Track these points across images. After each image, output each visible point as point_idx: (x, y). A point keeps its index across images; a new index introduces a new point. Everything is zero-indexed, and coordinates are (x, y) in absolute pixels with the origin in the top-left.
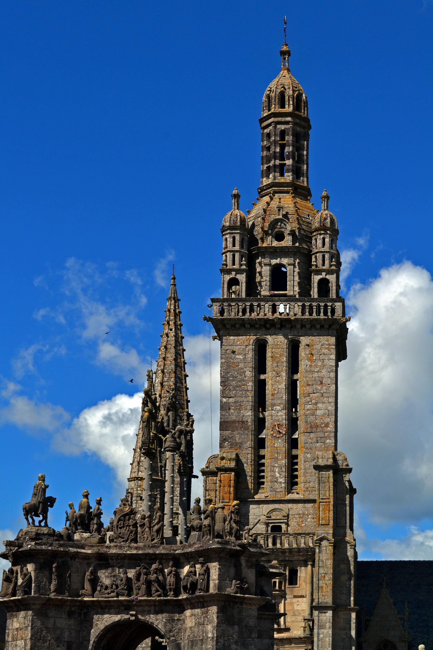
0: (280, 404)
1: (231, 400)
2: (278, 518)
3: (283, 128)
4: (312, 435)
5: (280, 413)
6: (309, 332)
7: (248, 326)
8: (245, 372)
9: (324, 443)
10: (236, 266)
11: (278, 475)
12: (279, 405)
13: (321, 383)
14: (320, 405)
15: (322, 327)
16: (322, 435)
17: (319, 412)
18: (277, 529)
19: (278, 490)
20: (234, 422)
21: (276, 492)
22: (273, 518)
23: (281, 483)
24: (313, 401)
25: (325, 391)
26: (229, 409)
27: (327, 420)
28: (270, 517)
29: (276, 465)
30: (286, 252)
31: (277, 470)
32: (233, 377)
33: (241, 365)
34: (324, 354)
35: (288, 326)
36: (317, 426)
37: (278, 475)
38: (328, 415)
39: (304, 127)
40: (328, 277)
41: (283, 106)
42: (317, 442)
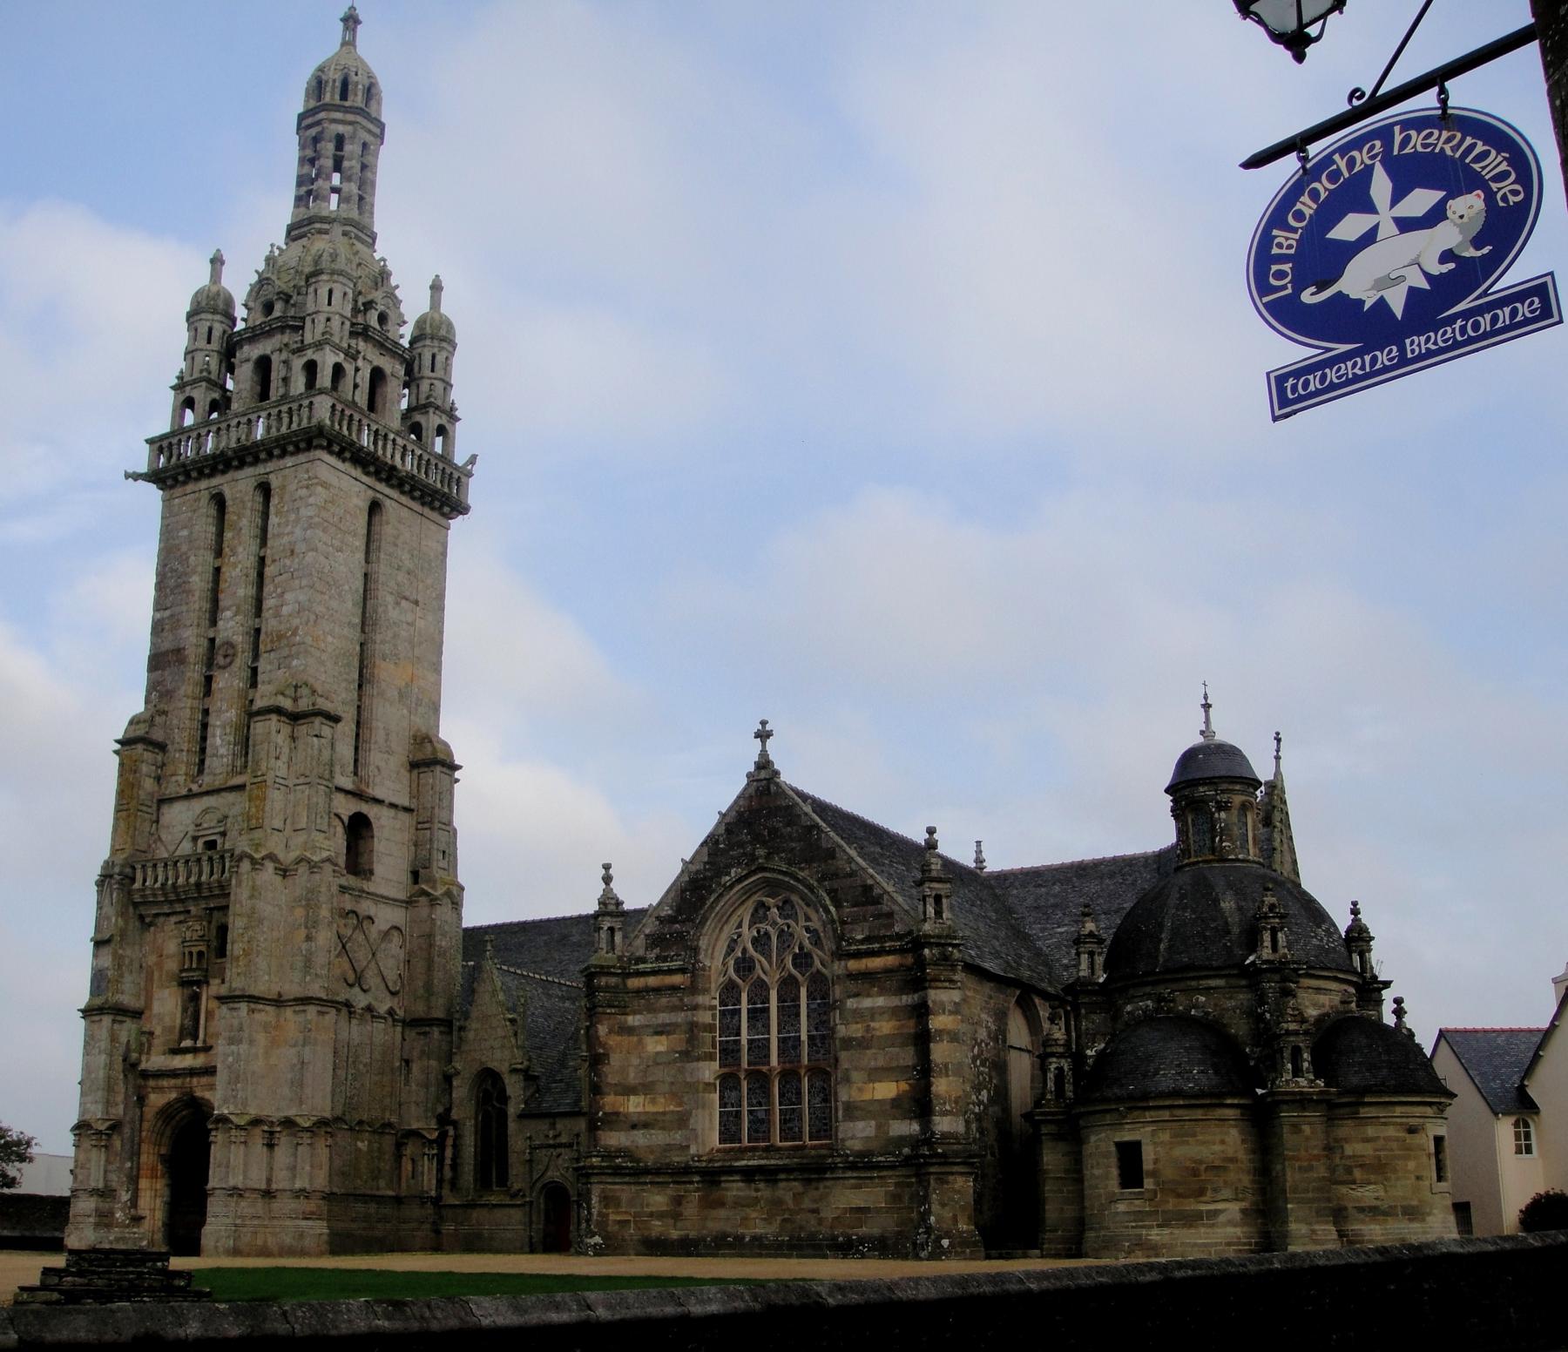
0: (231, 606)
1: (167, 613)
2: (212, 825)
3: (314, 134)
4: (272, 654)
5: (232, 623)
6: (282, 463)
7: (194, 474)
8: (188, 558)
9: (289, 667)
10: (196, 375)
11: (218, 741)
12: (228, 609)
13: (292, 552)
14: (289, 596)
15: (298, 451)
16: (285, 652)
17: (285, 610)
18: (211, 845)
19: (218, 771)
20: (166, 653)
21: (215, 775)
22: (205, 825)
23: (222, 756)
24: (279, 590)
25: (297, 566)
26: (163, 630)
27: (296, 622)
28: (200, 825)
29: (218, 723)
30: (268, 331)
31: (218, 733)
32: (172, 570)
33: (184, 548)
34: (301, 498)
35: (249, 459)
36: (280, 637)
37: (218, 741)
38: (299, 612)
39: (351, 123)
40: (314, 357)
41: (319, 99)
42: (279, 669)
